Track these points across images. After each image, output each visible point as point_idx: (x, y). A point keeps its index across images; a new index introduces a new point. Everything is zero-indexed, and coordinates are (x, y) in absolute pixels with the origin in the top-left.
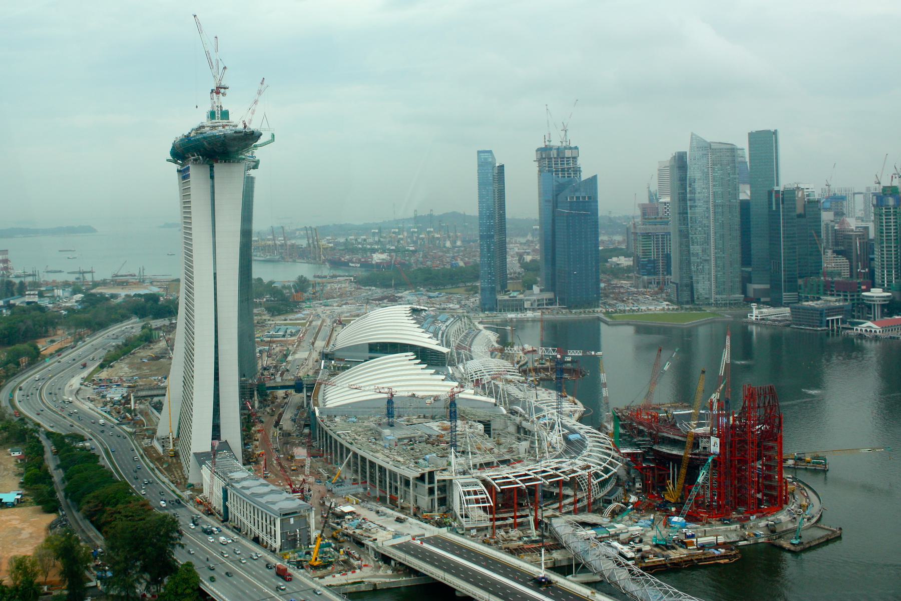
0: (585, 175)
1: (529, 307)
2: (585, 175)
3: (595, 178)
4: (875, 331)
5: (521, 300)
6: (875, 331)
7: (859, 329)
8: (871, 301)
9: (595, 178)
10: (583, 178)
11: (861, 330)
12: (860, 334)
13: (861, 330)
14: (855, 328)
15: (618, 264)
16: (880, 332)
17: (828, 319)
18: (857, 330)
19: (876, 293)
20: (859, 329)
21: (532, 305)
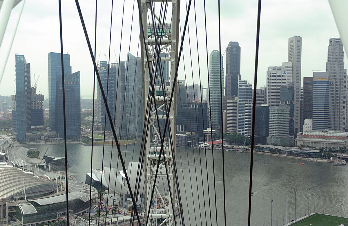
0: (73, 71)
1: (43, 138)
2: (73, 71)
3: (79, 72)
4: (208, 147)
5: (39, 135)
6: (208, 147)
7: (201, 146)
8: (207, 134)
9: (79, 72)
10: (72, 73)
11: (202, 146)
12: (202, 148)
13: (202, 146)
14: (200, 145)
15: (89, 120)
16: (210, 147)
17: (188, 142)
18: (200, 146)
19: (209, 130)
20: (201, 146)
21: (45, 137)
